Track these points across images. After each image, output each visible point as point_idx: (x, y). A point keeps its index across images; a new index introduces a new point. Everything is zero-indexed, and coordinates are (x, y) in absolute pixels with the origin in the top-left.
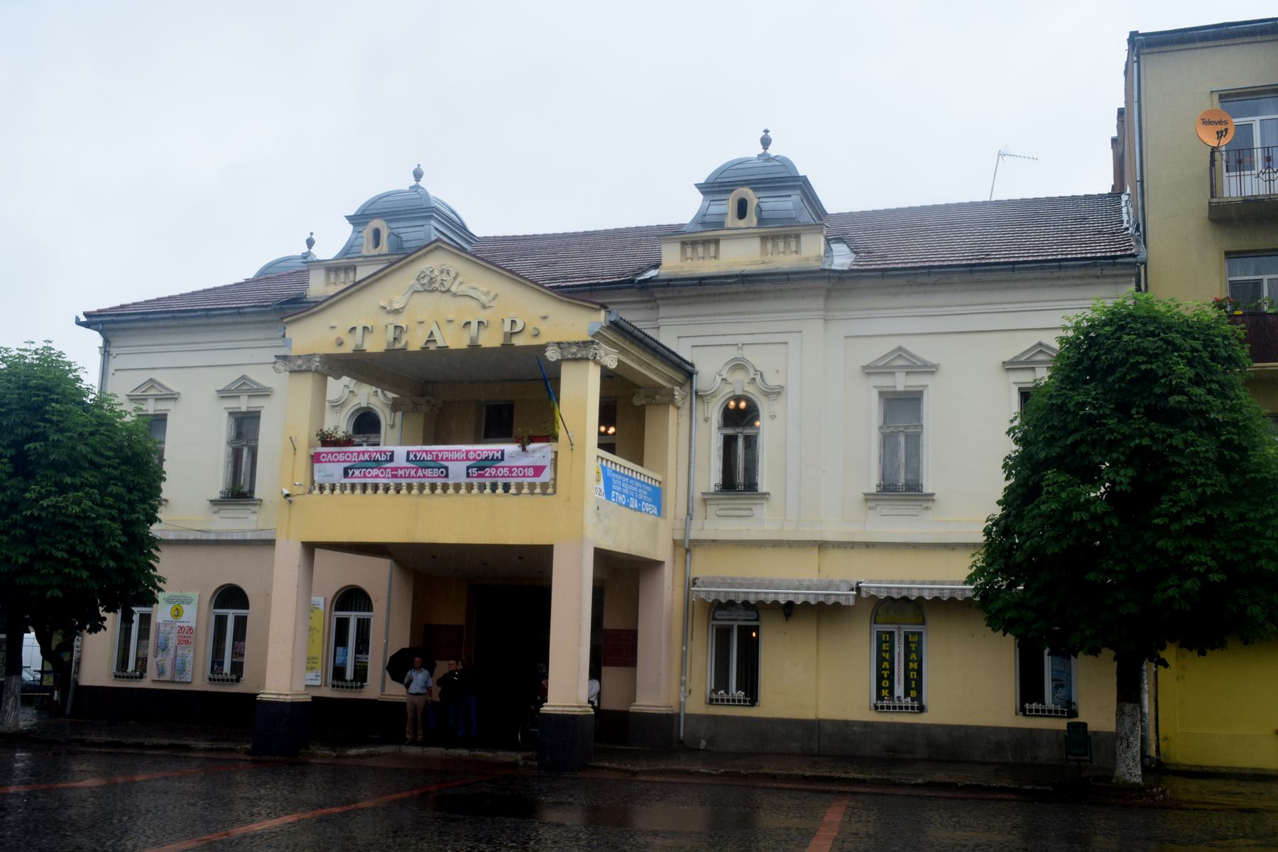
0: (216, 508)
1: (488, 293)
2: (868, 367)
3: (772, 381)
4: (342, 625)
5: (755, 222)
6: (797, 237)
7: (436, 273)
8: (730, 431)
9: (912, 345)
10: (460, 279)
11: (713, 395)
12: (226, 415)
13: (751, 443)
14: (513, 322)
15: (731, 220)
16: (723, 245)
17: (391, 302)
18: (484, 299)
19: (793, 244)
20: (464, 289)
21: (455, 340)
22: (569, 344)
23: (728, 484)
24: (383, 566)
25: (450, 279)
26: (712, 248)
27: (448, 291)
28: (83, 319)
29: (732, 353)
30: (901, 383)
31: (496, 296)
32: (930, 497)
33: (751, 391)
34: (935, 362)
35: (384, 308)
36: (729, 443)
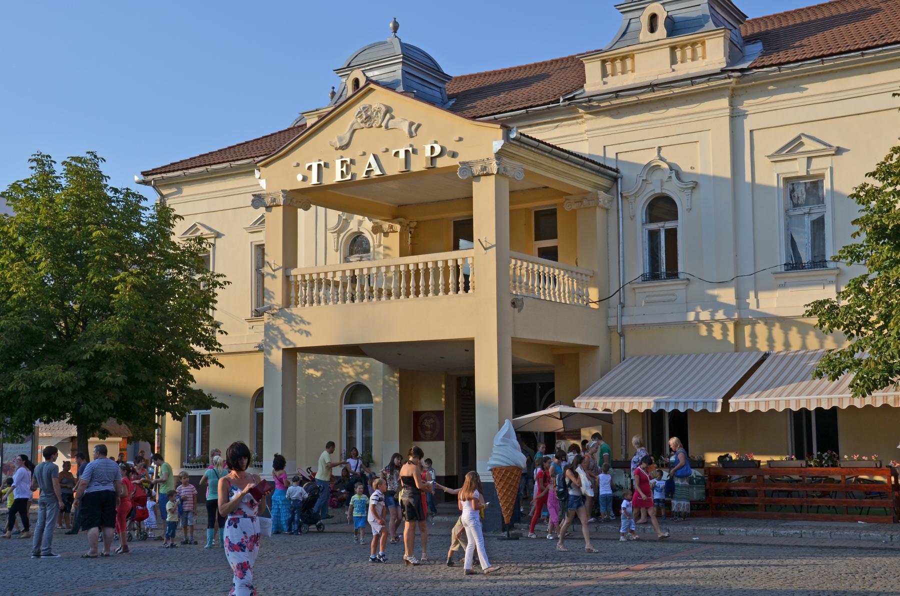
4: (351, 414)
6: (703, 43)
8: (654, 226)
11: (636, 195)
13: (672, 235)
15: (645, 35)
16: (636, 56)
24: (368, 362)
26: (628, 62)
28: (142, 178)
33: (672, 190)
36: (653, 236)
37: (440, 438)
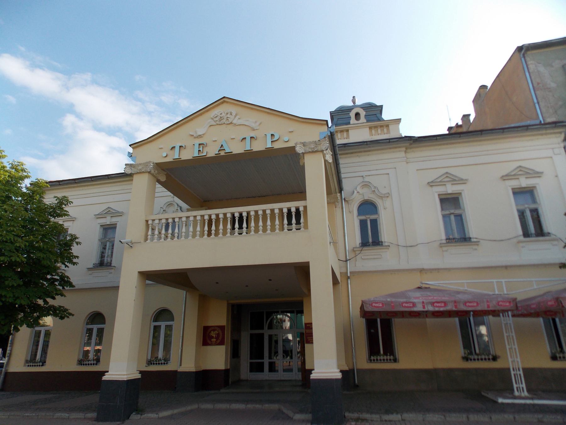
0: (90, 272)
1: (256, 122)
2: (432, 182)
3: (384, 191)
5: (365, 121)
6: (387, 126)
7: (223, 114)
9: (452, 171)
10: (238, 117)
12: (99, 226)
13: (375, 223)
14: (272, 135)
16: (351, 132)
17: (196, 132)
18: (253, 125)
19: (385, 130)
20: (240, 122)
21: (237, 148)
22: (310, 143)
23: (364, 244)
25: (233, 117)
26: (345, 134)
27: (231, 123)
29: (361, 179)
30: (450, 189)
31: (260, 124)
32: (477, 243)
34: (464, 178)
35: (193, 136)
36: (363, 224)
37: (222, 343)
